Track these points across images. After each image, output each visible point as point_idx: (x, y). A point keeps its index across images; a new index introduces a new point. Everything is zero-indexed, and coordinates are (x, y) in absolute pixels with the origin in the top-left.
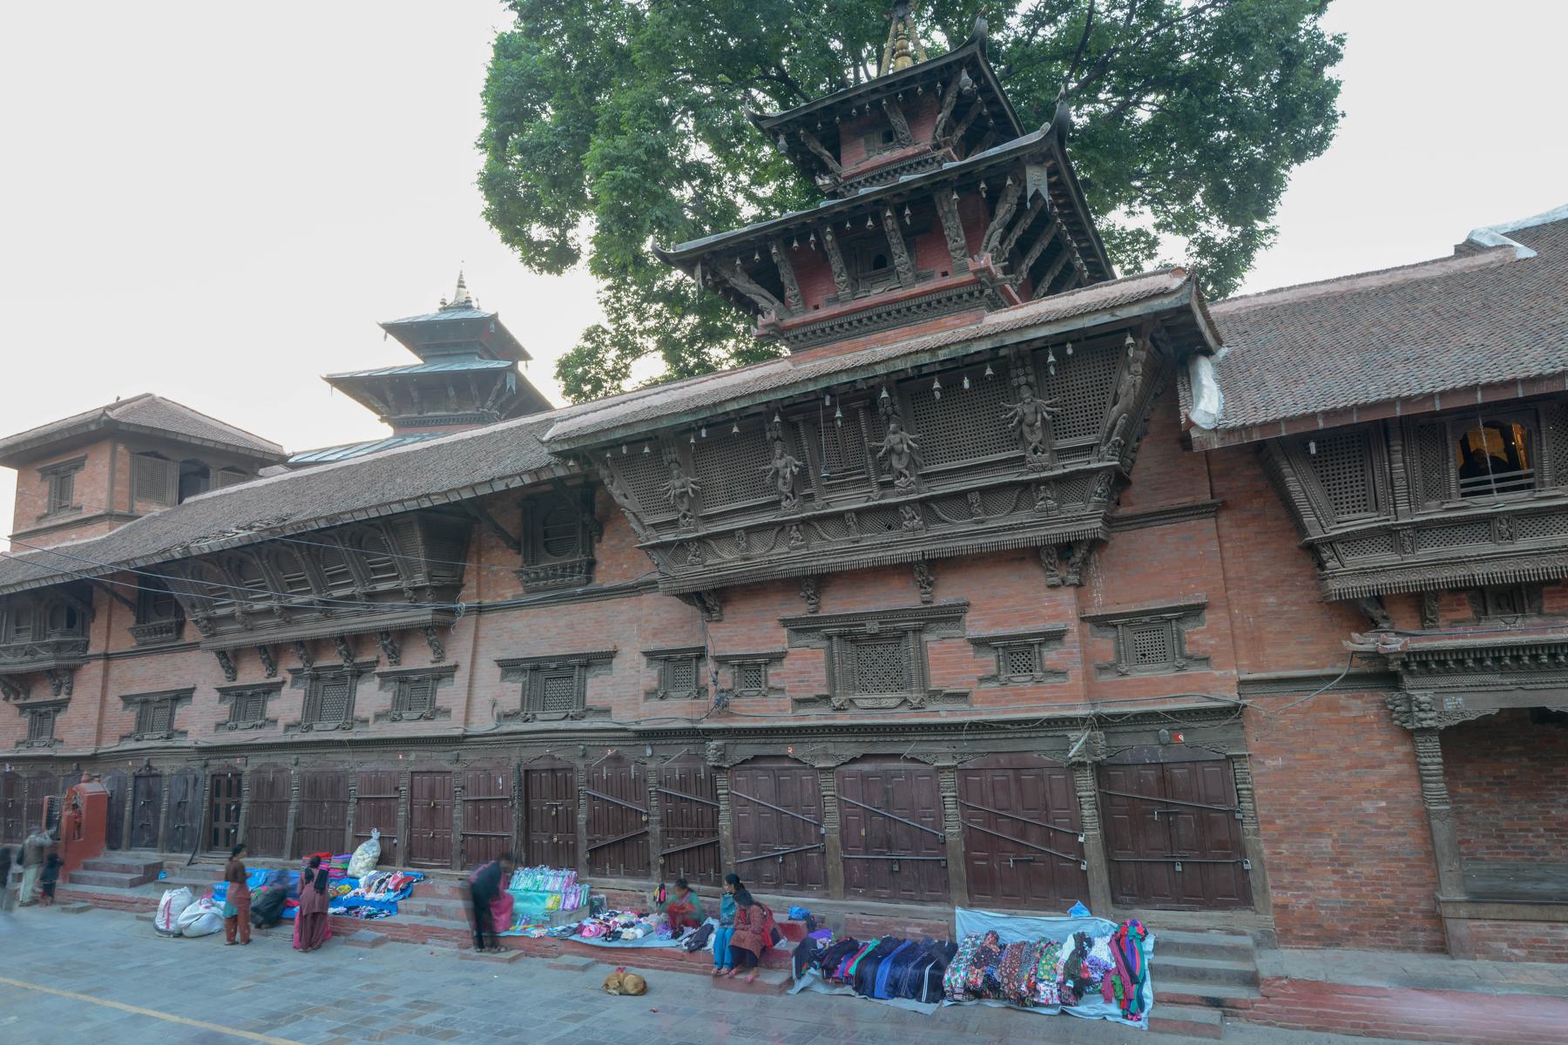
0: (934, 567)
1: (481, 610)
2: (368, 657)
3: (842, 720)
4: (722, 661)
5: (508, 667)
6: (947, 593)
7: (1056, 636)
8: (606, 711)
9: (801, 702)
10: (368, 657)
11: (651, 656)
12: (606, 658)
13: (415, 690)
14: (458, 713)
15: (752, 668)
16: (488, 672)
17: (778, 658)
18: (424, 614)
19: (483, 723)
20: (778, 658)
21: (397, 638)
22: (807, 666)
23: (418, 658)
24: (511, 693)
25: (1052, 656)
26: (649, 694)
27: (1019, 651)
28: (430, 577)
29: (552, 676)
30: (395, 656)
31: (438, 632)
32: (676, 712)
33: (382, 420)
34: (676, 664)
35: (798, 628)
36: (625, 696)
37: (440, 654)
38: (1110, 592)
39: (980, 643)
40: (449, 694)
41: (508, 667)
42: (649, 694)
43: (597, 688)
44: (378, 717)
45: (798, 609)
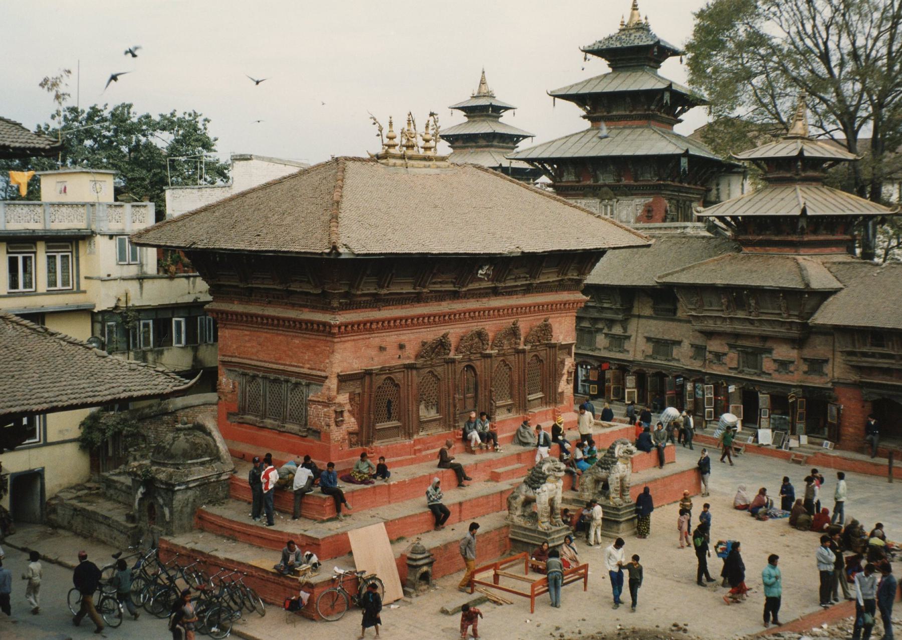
0: (765, 338)
1: (639, 317)
2: (600, 326)
3: (740, 376)
4: (710, 352)
5: (649, 339)
6: (768, 345)
7: (792, 362)
8: (678, 360)
9: (731, 368)
10: (600, 326)
11: (692, 345)
12: (679, 343)
13: (618, 341)
14: (632, 353)
15: (718, 356)
16: (641, 341)
17: (725, 354)
18: (620, 317)
19: (639, 357)
20: (725, 354)
21: (611, 323)
22: (732, 358)
23: (617, 330)
24: (649, 348)
25: (792, 368)
26: (691, 357)
27: (783, 365)
28: (622, 305)
29: (662, 345)
30: (610, 328)
31: (624, 323)
32: (696, 365)
33: (584, 117)
34: (699, 351)
35: (731, 346)
36: (683, 358)
37: (625, 330)
38: (808, 353)
39: (775, 361)
40: (627, 345)
41: (649, 339)
42: (691, 357)
43: (676, 352)
44: (604, 348)
45: (732, 342)
